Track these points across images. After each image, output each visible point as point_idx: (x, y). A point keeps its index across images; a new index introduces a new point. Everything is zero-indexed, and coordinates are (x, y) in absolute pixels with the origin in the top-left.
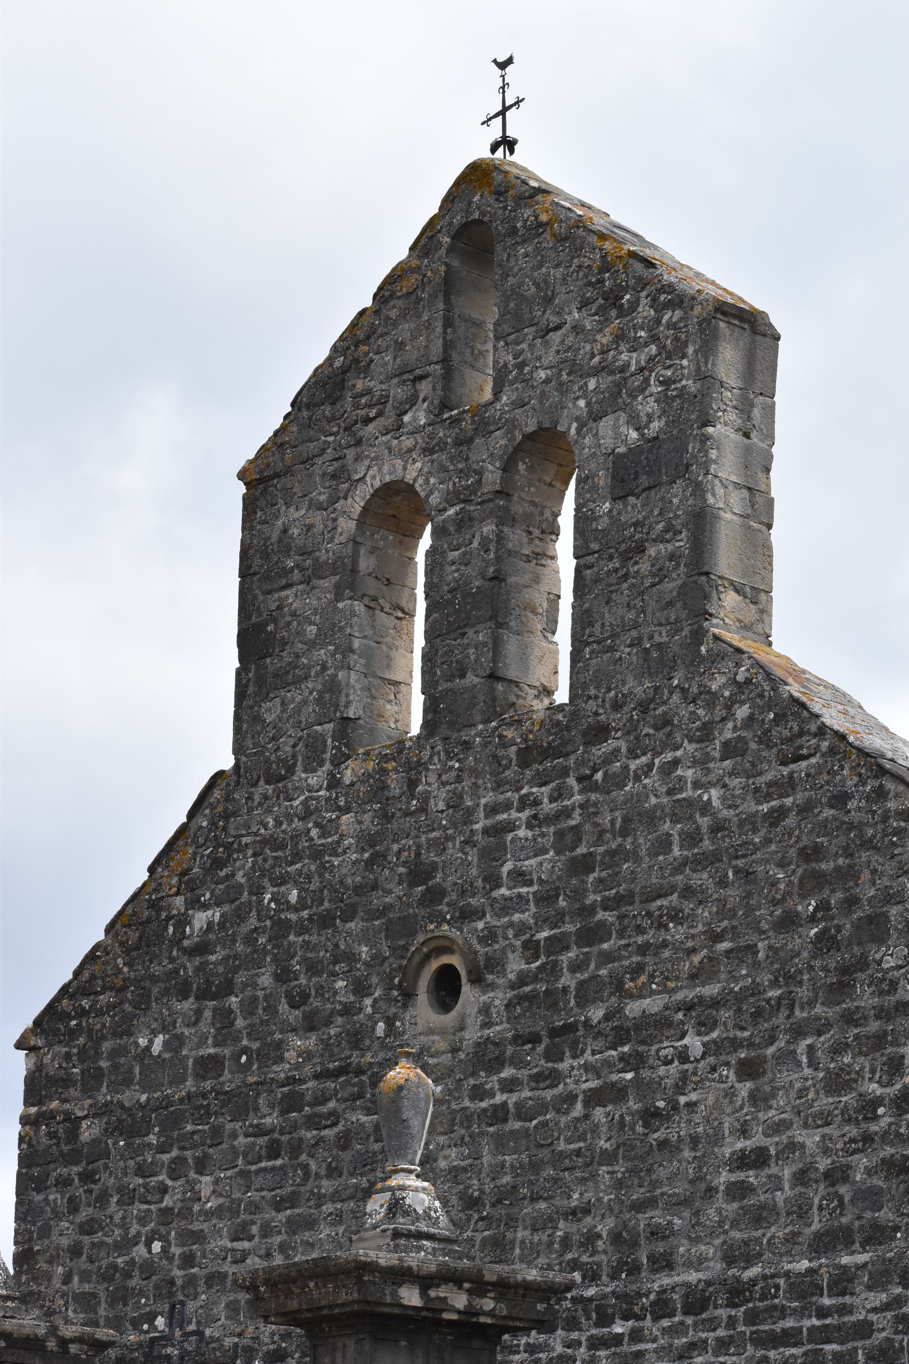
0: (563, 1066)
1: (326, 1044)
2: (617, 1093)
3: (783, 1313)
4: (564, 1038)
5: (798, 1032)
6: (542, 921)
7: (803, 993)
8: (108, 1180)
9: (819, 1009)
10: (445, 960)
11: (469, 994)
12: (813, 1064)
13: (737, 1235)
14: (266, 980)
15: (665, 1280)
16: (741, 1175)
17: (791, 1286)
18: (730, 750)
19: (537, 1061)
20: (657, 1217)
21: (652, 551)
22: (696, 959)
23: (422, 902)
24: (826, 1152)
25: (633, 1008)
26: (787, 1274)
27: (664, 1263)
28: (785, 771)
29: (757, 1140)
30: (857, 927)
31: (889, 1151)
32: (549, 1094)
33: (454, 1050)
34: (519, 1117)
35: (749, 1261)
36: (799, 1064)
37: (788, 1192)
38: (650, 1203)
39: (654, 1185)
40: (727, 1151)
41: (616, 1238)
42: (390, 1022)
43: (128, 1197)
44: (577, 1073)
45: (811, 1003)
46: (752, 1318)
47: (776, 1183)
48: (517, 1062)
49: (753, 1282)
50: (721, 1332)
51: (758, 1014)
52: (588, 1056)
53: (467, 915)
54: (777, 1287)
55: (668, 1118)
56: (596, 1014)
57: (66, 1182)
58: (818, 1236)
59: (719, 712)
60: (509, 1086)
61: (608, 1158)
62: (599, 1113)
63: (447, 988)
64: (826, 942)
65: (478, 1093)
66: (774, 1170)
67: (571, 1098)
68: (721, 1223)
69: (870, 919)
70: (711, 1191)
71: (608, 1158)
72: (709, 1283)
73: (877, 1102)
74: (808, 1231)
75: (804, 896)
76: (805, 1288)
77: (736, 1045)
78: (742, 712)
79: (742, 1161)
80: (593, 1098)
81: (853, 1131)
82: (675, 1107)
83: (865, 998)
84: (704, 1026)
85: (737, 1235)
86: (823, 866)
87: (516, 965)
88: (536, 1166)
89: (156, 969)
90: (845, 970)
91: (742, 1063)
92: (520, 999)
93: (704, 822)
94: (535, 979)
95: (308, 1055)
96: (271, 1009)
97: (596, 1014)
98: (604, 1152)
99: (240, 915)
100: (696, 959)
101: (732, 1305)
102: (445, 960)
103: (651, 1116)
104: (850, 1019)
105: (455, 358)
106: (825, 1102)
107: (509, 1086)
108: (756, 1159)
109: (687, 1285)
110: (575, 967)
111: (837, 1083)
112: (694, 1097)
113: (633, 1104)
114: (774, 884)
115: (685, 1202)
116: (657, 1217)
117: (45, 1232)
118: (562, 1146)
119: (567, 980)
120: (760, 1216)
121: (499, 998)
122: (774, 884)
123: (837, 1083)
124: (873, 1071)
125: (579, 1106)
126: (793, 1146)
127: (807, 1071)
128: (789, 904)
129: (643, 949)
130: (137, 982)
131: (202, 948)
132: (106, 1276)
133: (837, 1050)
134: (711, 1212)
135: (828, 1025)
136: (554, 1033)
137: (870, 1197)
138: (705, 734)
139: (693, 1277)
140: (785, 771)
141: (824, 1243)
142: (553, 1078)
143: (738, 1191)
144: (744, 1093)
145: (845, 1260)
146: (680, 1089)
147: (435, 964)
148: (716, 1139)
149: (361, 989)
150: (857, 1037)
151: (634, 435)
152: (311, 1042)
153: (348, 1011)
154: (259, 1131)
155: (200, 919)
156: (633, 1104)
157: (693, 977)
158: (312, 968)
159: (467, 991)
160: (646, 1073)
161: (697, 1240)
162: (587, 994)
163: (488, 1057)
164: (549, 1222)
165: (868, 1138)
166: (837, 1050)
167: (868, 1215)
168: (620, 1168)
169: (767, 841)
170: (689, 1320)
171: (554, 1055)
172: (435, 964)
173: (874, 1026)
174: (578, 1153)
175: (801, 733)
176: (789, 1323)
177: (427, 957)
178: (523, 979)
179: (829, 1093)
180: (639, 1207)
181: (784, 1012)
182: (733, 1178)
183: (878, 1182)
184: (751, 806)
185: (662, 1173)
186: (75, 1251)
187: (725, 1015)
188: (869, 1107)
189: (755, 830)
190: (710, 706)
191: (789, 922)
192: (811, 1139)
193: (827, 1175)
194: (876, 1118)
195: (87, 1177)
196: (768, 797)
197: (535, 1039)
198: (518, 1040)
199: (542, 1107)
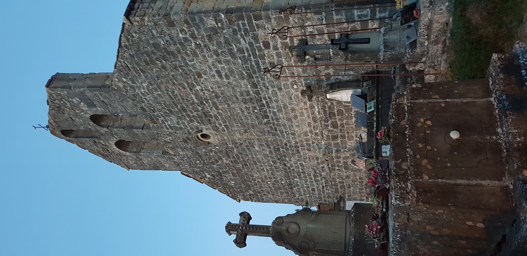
0: (213, 114)
1: (223, 156)
2: (214, 103)
3: (252, 65)
4: (206, 114)
5: (187, 65)
6: (185, 119)
7: (178, 63)
8: (259, 190)
9: (180, 59)
10: (200, 137)
11: (205, 132)
12: (193, 60)
13: (237, 77)
14: (215, 166)
15: (251, 92)
16: (224, 76)
17: (245, 64)
18: (133, 82)
19: (213, 119)
20: (238, 94)
21: (102, 99)
22: (181, 88)
23: (191, 141)
24: (212, 56)
25: (196, 101)
26: (242, 65)
27: (248, 93)
28: (132, 70)
29: (214, 73)
30: (158, 51)
31: (206, 40)
32: (219, 117)
33: (217, 135)
34: (226, 123)
35: (243, 74)
36: (194, 64)
37: (224, 65)
38: (235, 96)
39: (232, 95)
40: (219, 80)
41: (245, 103)
42: (215, 146)
43: (261, 187)
44: (214, 112)
45: (179, 61)
46: (255, 72)
47: (223, 68)
48: (215, 123)
49: (246, 73)
50: (260, 80)
51: (186, 74)
52: (209, 110)
53: (190, 133)
54: (246, 67)
55: (216, 93)
56: (200, 108)
57: (261, 196)
58: (232, 57)
59: (126, 84)
60: (221, 125)
61: (228, 105)
62: (220, 107)
63: (204, 136)
64: (164, 58)
65: (224, 130)
66: (220, 69)
67: (218, 113)
68: (236, 81)
69: (155, 48)
70: (229, 83)
71: (228, 105)
72: (249, 83)
73: (196, 43)
74: (232, 60)
75: (157, 64)
76: (245, 60)
77: (195, 79)
78: (124, 80)
79: (220, 76)
80: (217, 108)
81: (205, 50)
82: (213, 92)
83: (173, 48)
84: (194, 86)
85: (237, 77)
86: (148, 60)
87: (196, 124)
88: (235, 120)
89: (220, 182)
90: (168, 53)
91: (199, 77)
92: (203, 123)
93: (151, 87)
94: (197, 120)
95: (226, 159)
96: (220, 165)
97: (200, 108)
98: (228, 106)
99: (205, 170)
100: (181, 88)
101: (253, 77)
102: (200, 137)
103: (217, 96)
104: (179, 52)
105: (90, 136)
106: (200, 57)
107: (221, 125)
108: (218, 72)
109: (251, 88)
110: (192, 113)
111: (195, 55)
112: (210, 88)
113: (216, 100)
114: (157, 71)
115: (233, 88)
116: (238, 94)
117: (271, 199)
118: (229, 114)
119: (195, 114)
120: (232, 72)
121: (203, 127)
122: (157, 71)
123: (195, 55)
124: (189, 45)
125: (220, 111)
126: (213, 65)
127: (195, 62)
128: (160, 67)
129: (183, 99)
130: (223, 185)
131: (213, 175)
132: (277, 190)
133: (188, 55)
134: (234, 83)
135: (182, 57)
136: (206, 116)
137: (219, 44)
138: (132, 87)
139: (249, 86)
140: (132, 70)
141: (233, 56)
142: (216, 116)
143: (227, 77)
144: (205, 76)
145: (235, 50)
146: (209, 91)
147: (201, 138)
148: (217, 82)
149: (211, 151)
150: (183, 50)
151: (82, 103)
152: (224, 159)
153: (216, 153)
154: (243, 167)
155: (208, 176)
156: (216, 100)
157: (184, 89)
158: (210, 159)
159: (204, 133)
160: (208, 98)
161: (241, 86)
162: (197, 111)
163: (216, 129)
164: (245, 116)
165: (205, 46)
166: (188, 55)
167: (223, 45)
168: (230, 103)
169: (148, 73)
170: (259, 87)
171: (211, 116)
172: (201, 138)
173: (179, 46)
174: (230, 111)
175: (122, 66)
176: (254, 63)
177: (200, 140)
178: (198, 122)
179: (198, 57)
180: (237, 99)
181: (183, 68)
182: (225, 78)
183: (215, 43)
184: (143, 77)
185: (228, 94)
186: (273, 195)
187: (189, 81)
188: (198, 46)
189: (148, 76)
190: (127, 87)
191: (164, 67)
192: (210, 61)
193: (217, 56)
194: (200, 44)
195: (259, 193)
196: (139, 73)
197: (209, 120)
198: (210, 123)
199: (222, 118)
